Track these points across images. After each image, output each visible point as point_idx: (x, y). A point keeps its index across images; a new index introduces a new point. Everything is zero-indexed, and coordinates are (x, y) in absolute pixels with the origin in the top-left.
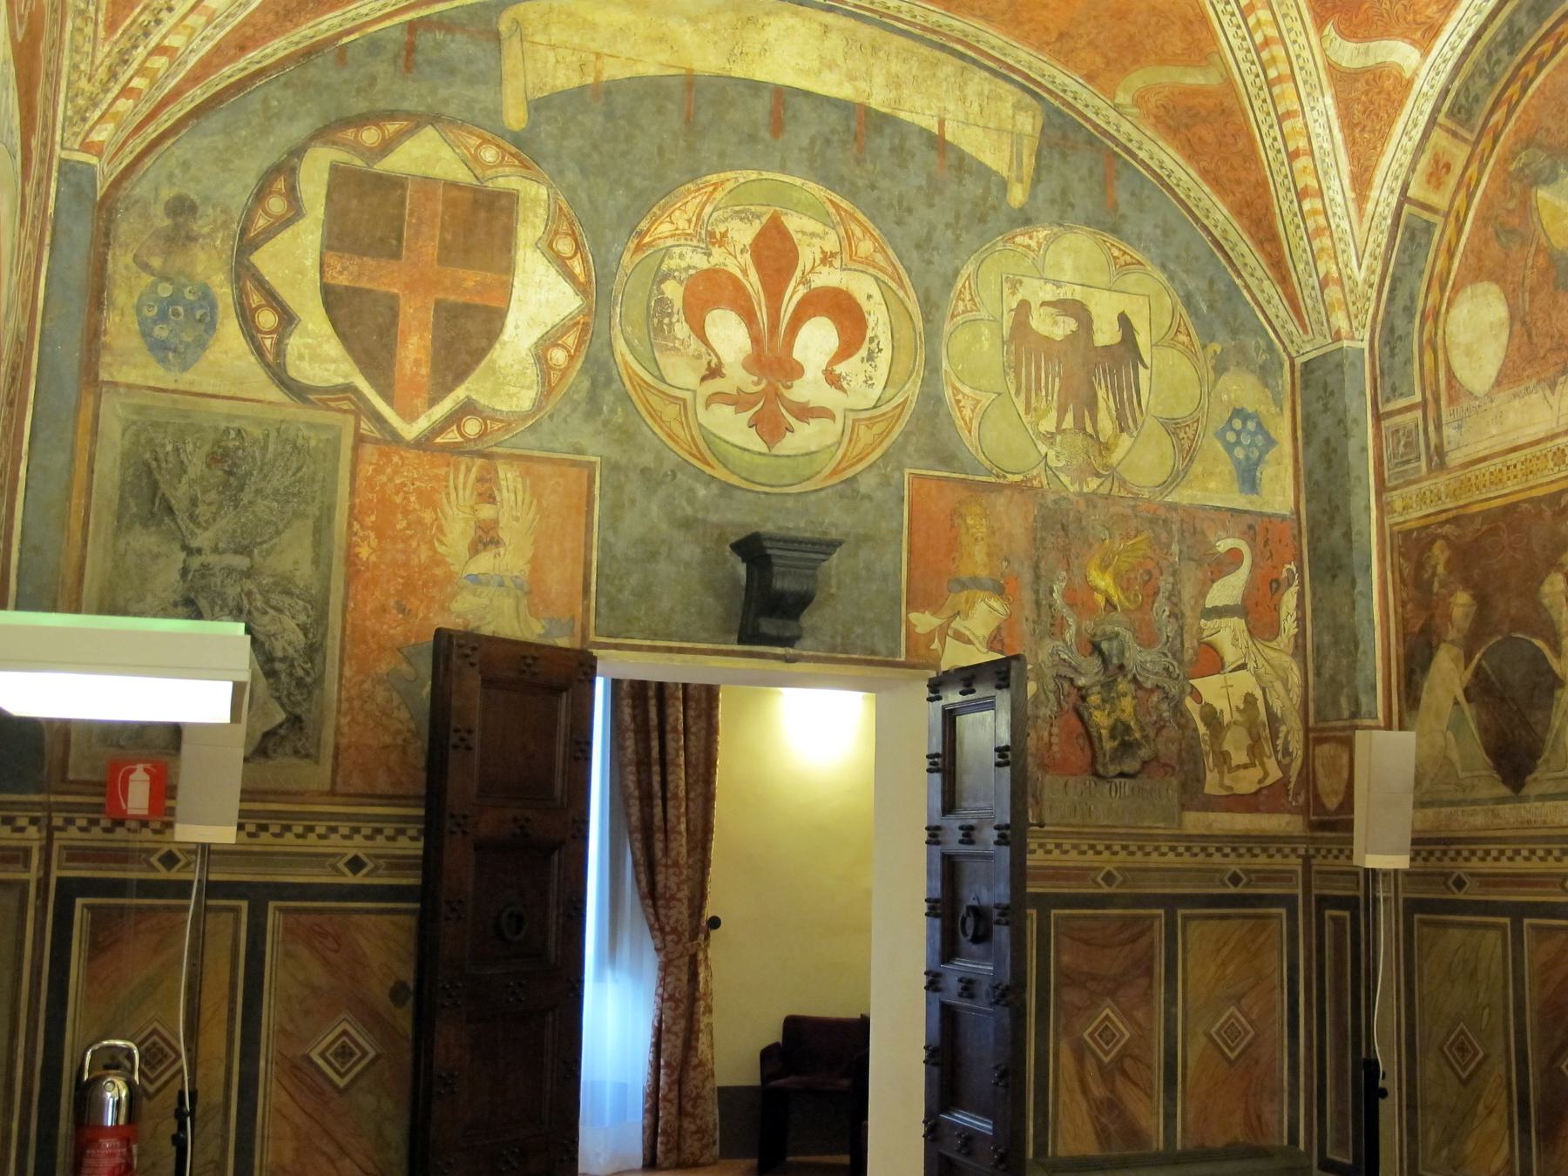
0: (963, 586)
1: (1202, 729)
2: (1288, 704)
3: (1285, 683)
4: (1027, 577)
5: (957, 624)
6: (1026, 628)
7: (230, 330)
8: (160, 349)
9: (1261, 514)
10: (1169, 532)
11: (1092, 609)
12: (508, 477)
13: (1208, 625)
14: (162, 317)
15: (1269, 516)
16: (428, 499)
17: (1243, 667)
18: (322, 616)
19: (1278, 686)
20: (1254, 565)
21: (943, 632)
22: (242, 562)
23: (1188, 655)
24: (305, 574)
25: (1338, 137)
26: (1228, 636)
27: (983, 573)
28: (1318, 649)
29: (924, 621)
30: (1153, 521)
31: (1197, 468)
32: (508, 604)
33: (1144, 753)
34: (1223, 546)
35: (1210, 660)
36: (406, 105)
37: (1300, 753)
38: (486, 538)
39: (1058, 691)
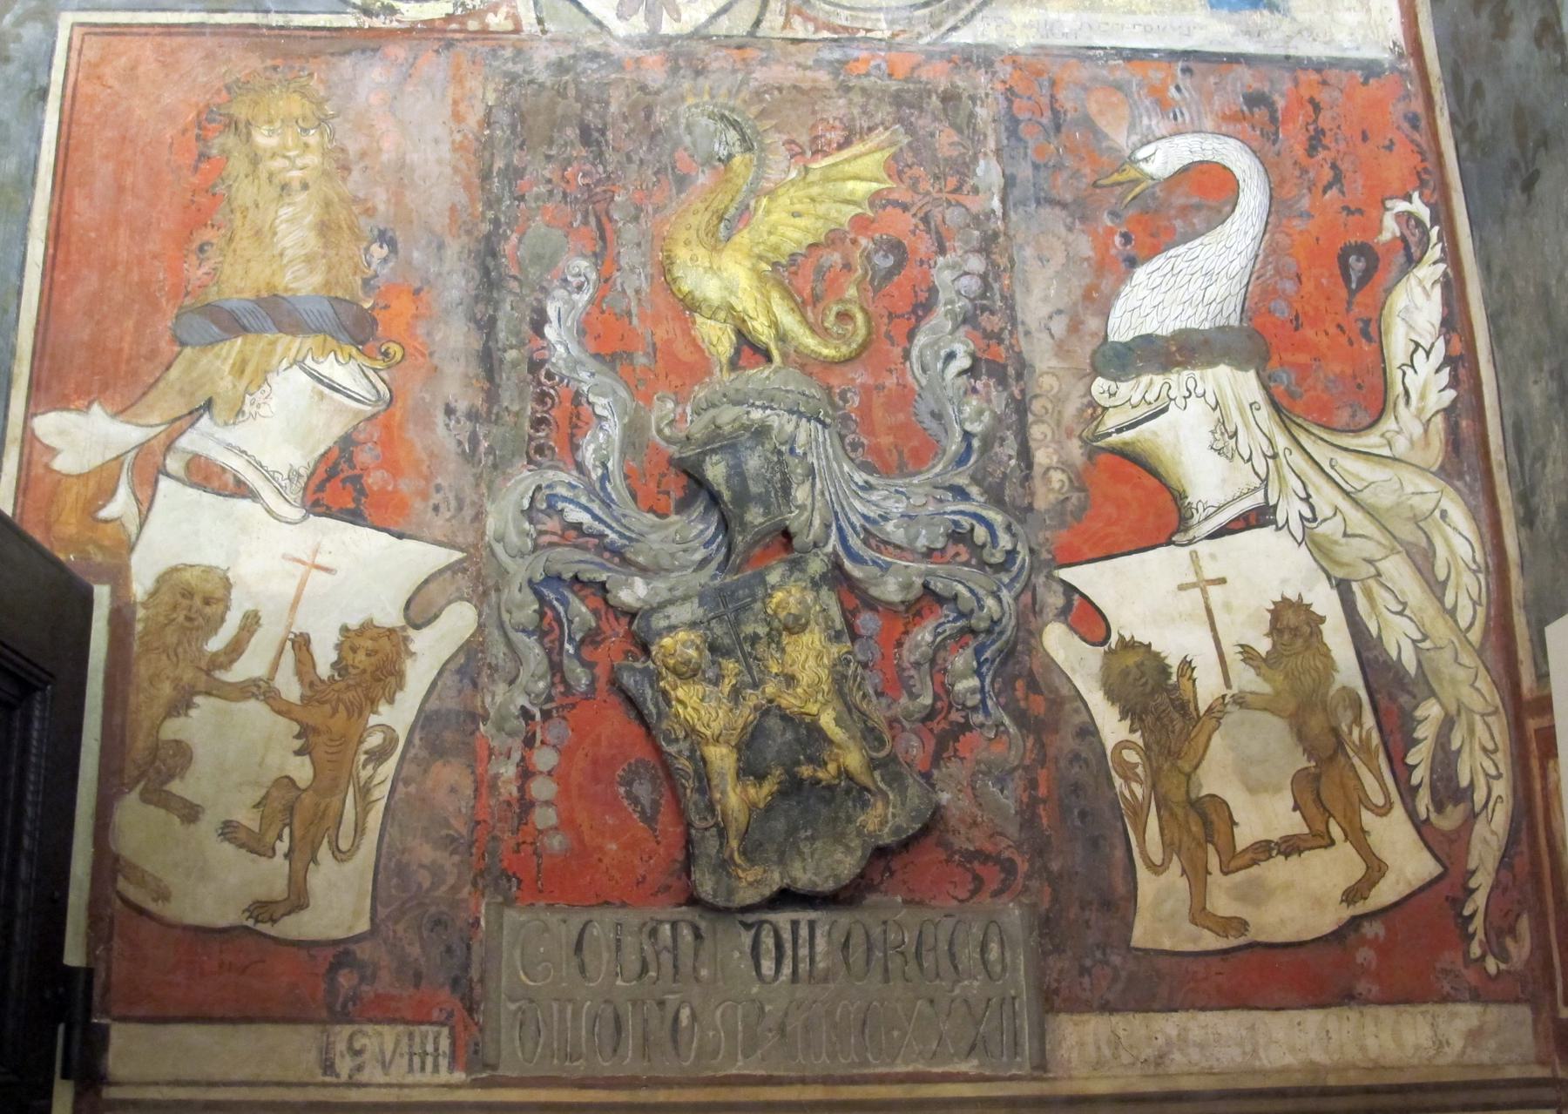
0: (231, 323)
1: (1112, 727)
2: (1441, 630)
3: (1422, 560)
4: (456, 284)
5: (203, 439)
6: (445, 436)
9: (1291, 64)
10: (968, 128)
11: (688, 368)
13: (1123, 397)
15: (1319, 66)
17: (1260, 517)
19: (1397, 570)
20: (1277, 203)
21: (147, 469)
23: (1051, 487)
26: (1200, 429)
27: (301, 282)
28: (1518, 434)
29: (82, 437)
30: (906, 101)
33: (882, 819)
34: (1163, 158)
35: (1140, 504)
37: (1501, 788)
39: (547, 628)
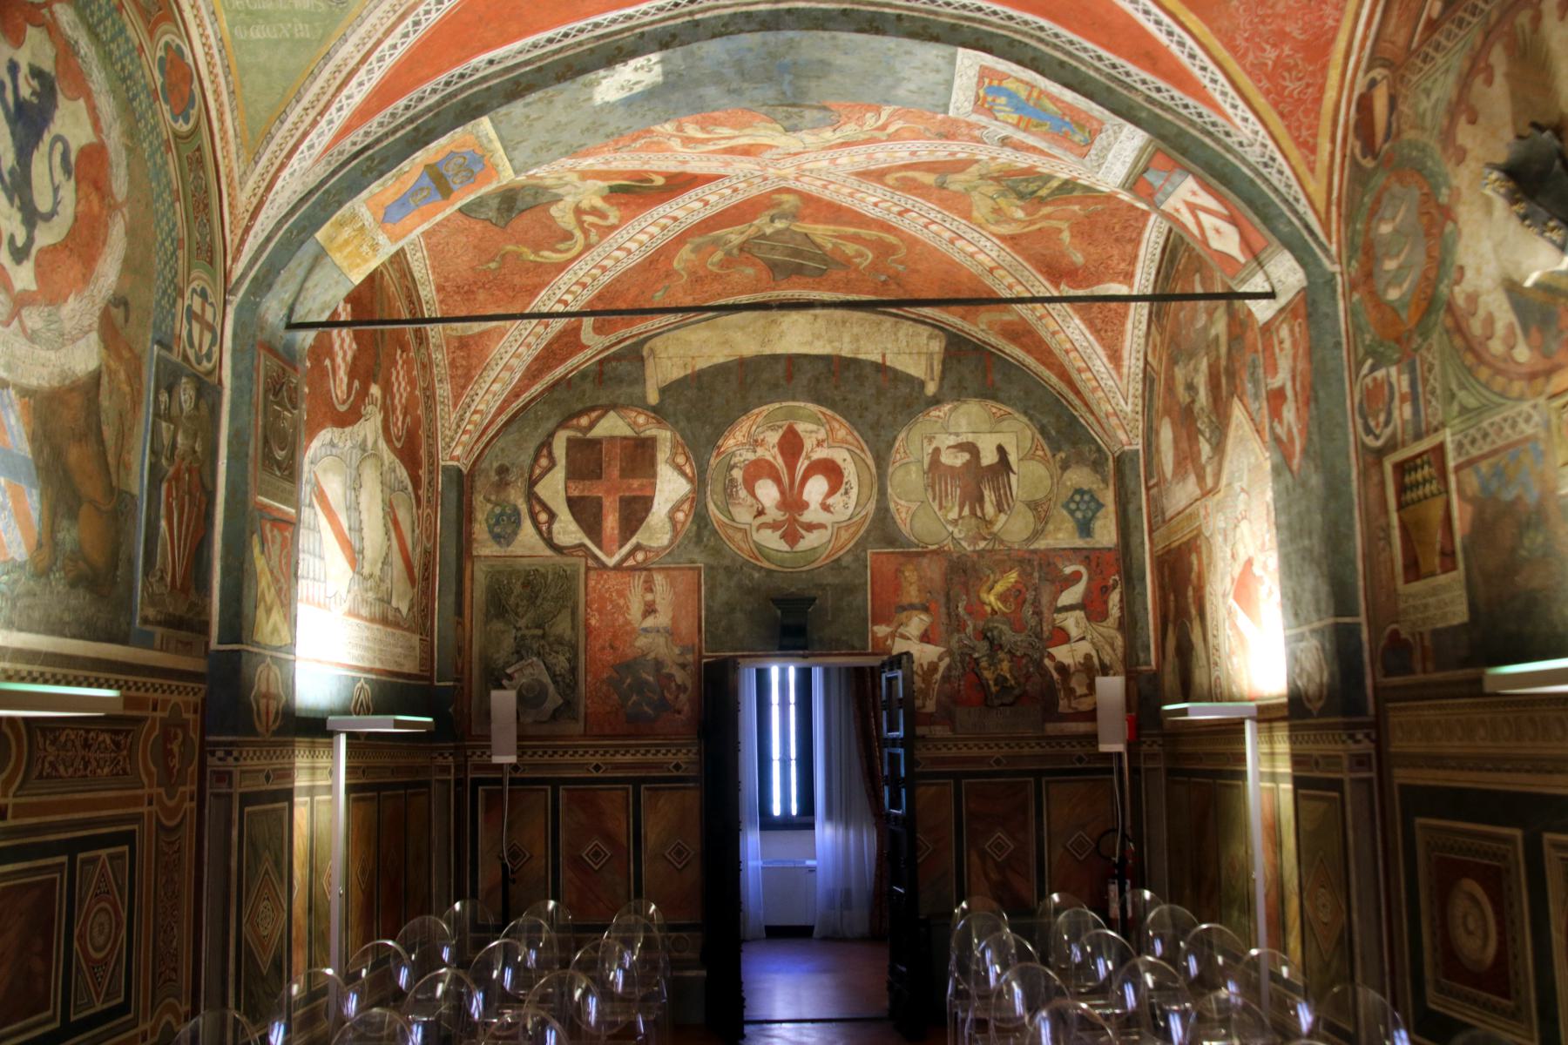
0: (903, 609)
1: (1055, 676)
3: (1112, 646)
4: (943, 600)
5: (902, 630)
6: (943, 628)
7: (527, 524)
8: (497, 538)
9: (1094, 549)
10: (1033, 566)
11: (984, 614)
12: (659, 579)
13: (1059, 617)
14: (497, 523)
16: (621, 594)
17: (1083, 638)
18: (576, 655)
19: (1107, 648)
20: (1090, 579)
21: (893, 635)
22: (539, 632)
23: (1046, 634)
24: (568, 634)
25: (1091, 338)
26: (1073, 622)
27: (916, 601)
29: (882, 630)
30: (1021, 562)
31: (1051, 527)
32: (662, 640)
33: (1017, 692)
34: (1068, 570)
35: (1063, 637)
36: (600, 402)
38: (650, 610)
39: (962, 662)
